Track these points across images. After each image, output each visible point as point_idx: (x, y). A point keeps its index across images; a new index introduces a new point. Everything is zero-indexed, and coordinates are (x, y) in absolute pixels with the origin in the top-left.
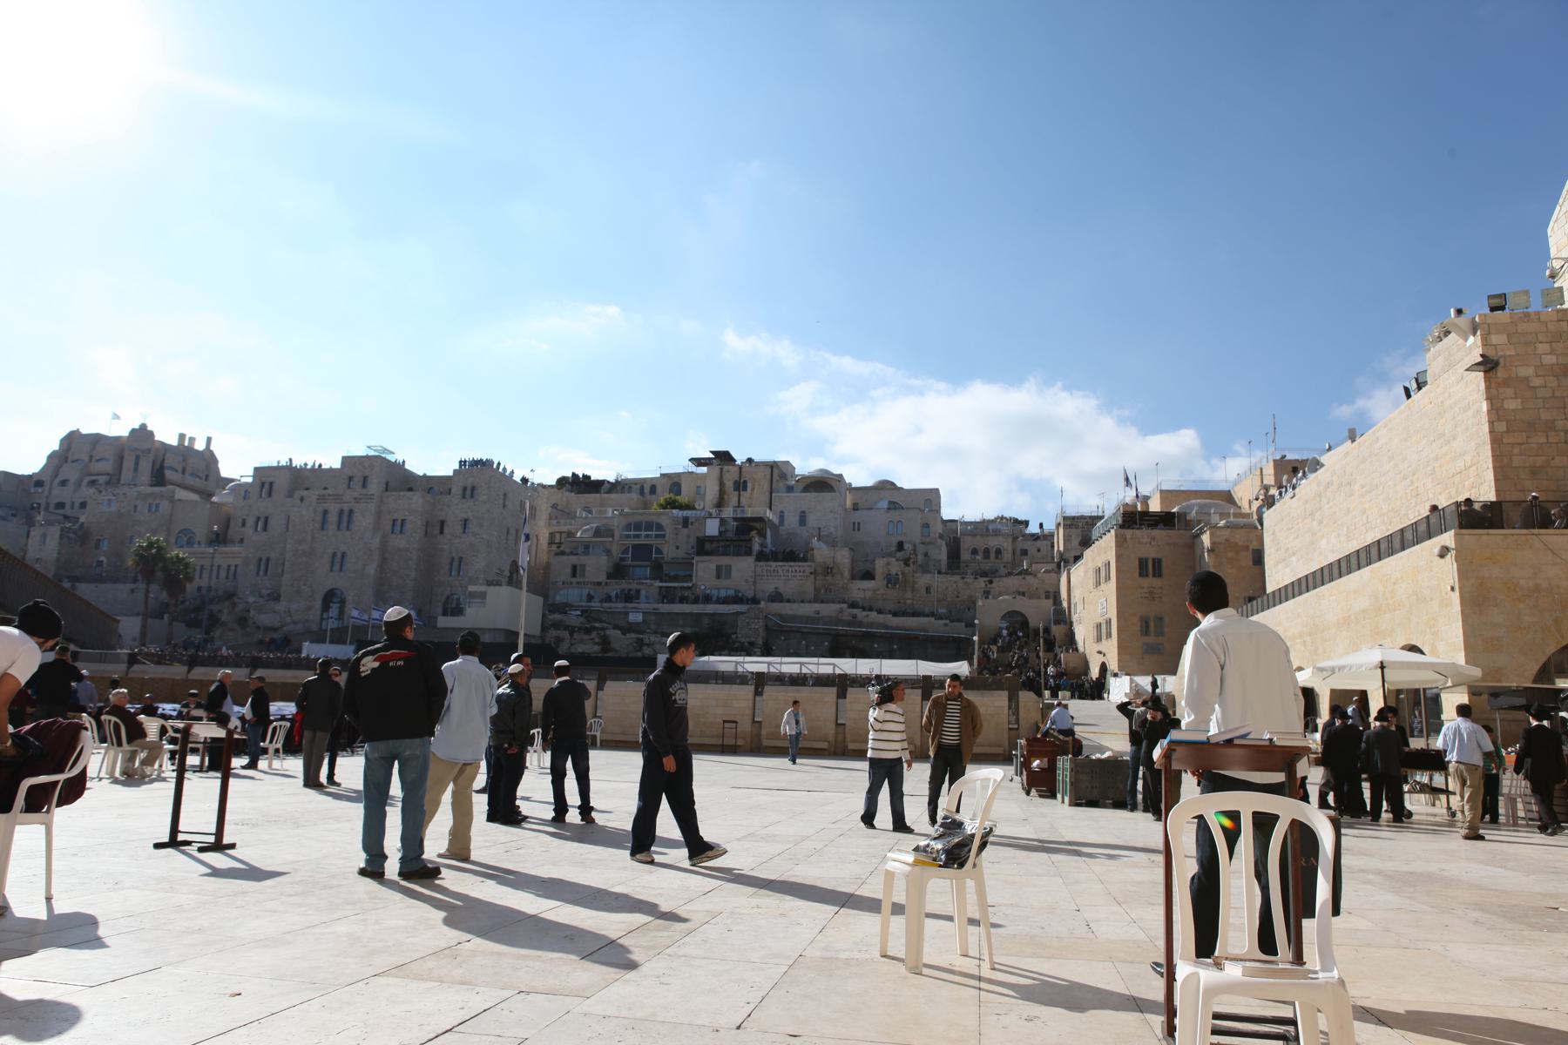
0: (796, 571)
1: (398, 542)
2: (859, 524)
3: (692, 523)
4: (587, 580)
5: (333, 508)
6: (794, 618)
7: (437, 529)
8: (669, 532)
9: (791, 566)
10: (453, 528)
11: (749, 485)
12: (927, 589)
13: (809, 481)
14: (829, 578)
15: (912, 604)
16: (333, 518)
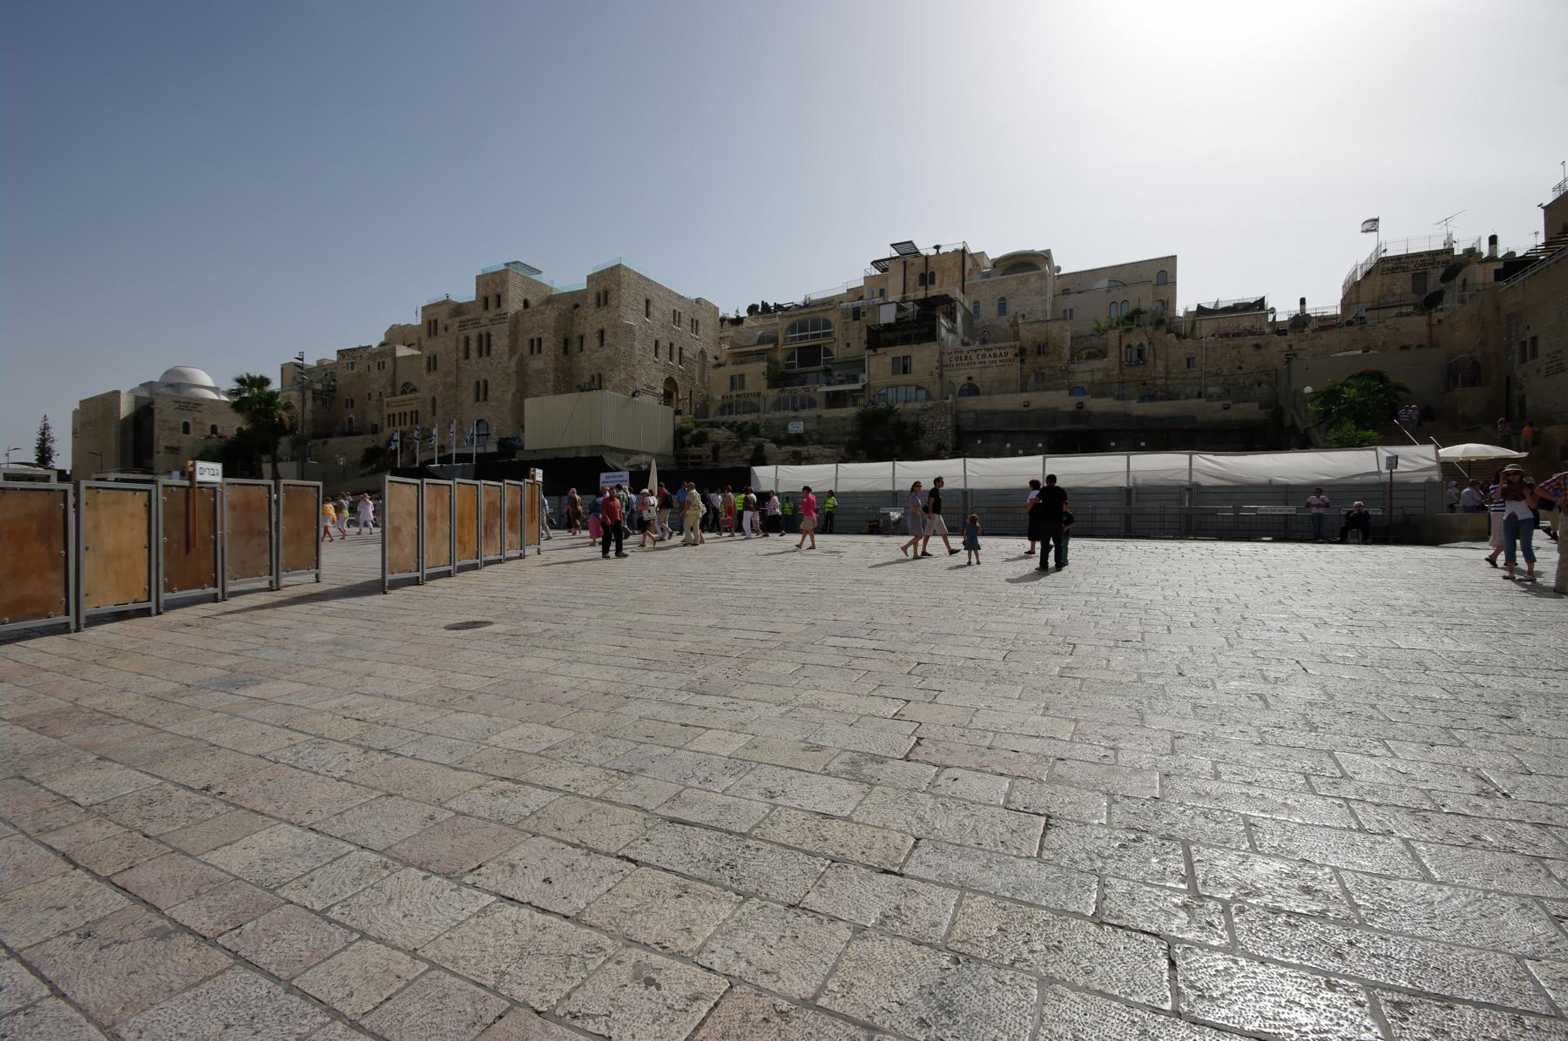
0: (995, 354)
1: (537, 363)
2: (1071, 310)
3: (864, 313)
4: (747, 391)
5: (473, 334)
6: (994, 413)
7: (577, 346)
8: (837, 329)
9: (988, 350)
10: (592, 342)
11: (938, 277)
12: (1188, 360)
13: (1008, 263)
14: (1042, 360)
15: (1166, 385)
16: (474, 345)
